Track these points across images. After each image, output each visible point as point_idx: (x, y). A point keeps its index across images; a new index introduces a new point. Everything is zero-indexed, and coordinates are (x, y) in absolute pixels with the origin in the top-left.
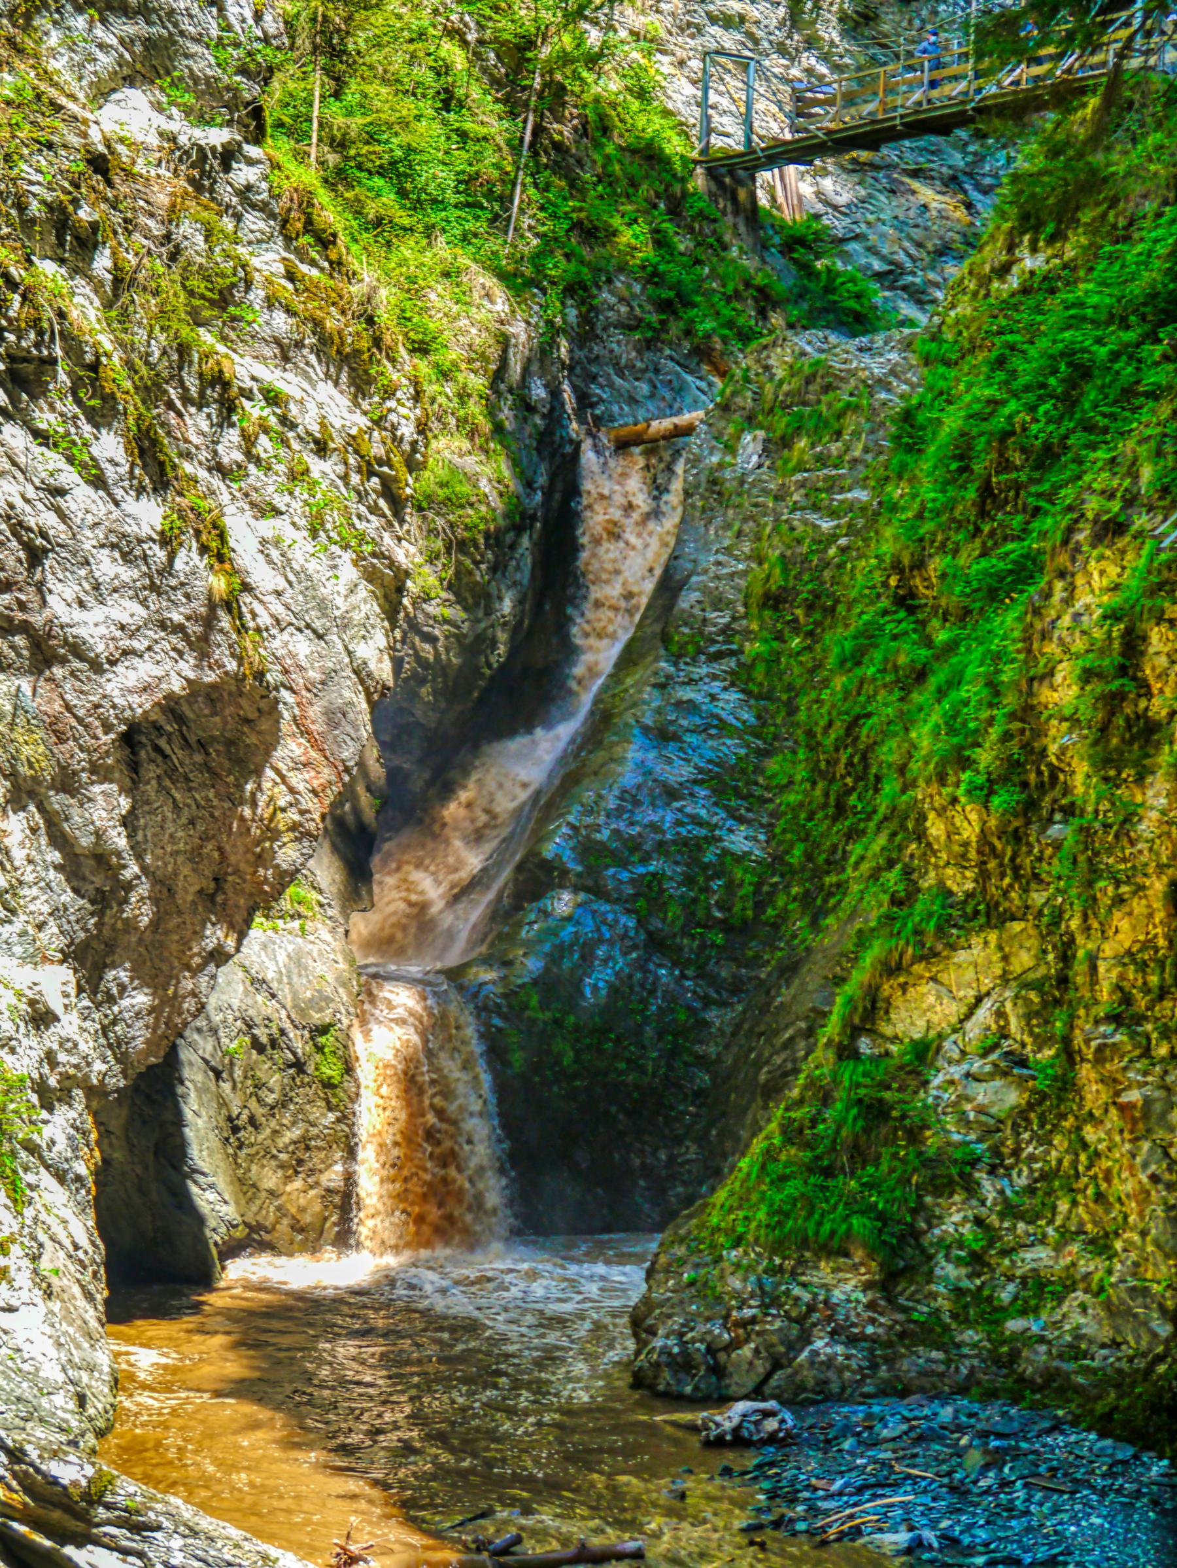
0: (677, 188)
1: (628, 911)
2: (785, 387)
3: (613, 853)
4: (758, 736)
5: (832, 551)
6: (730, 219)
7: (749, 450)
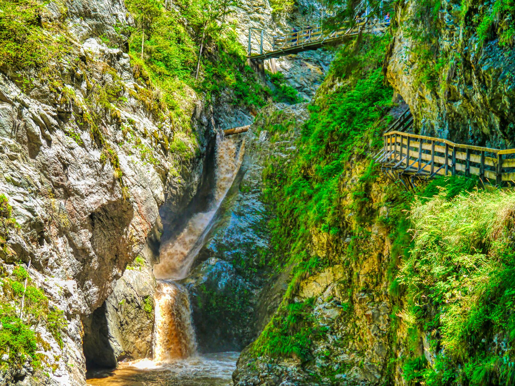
0: (242, 65)
1: (230, 263)
2: (272, 119)
3: (226, 247)
4: (266, 214)
5: (286, 163)
6: (257, 73)
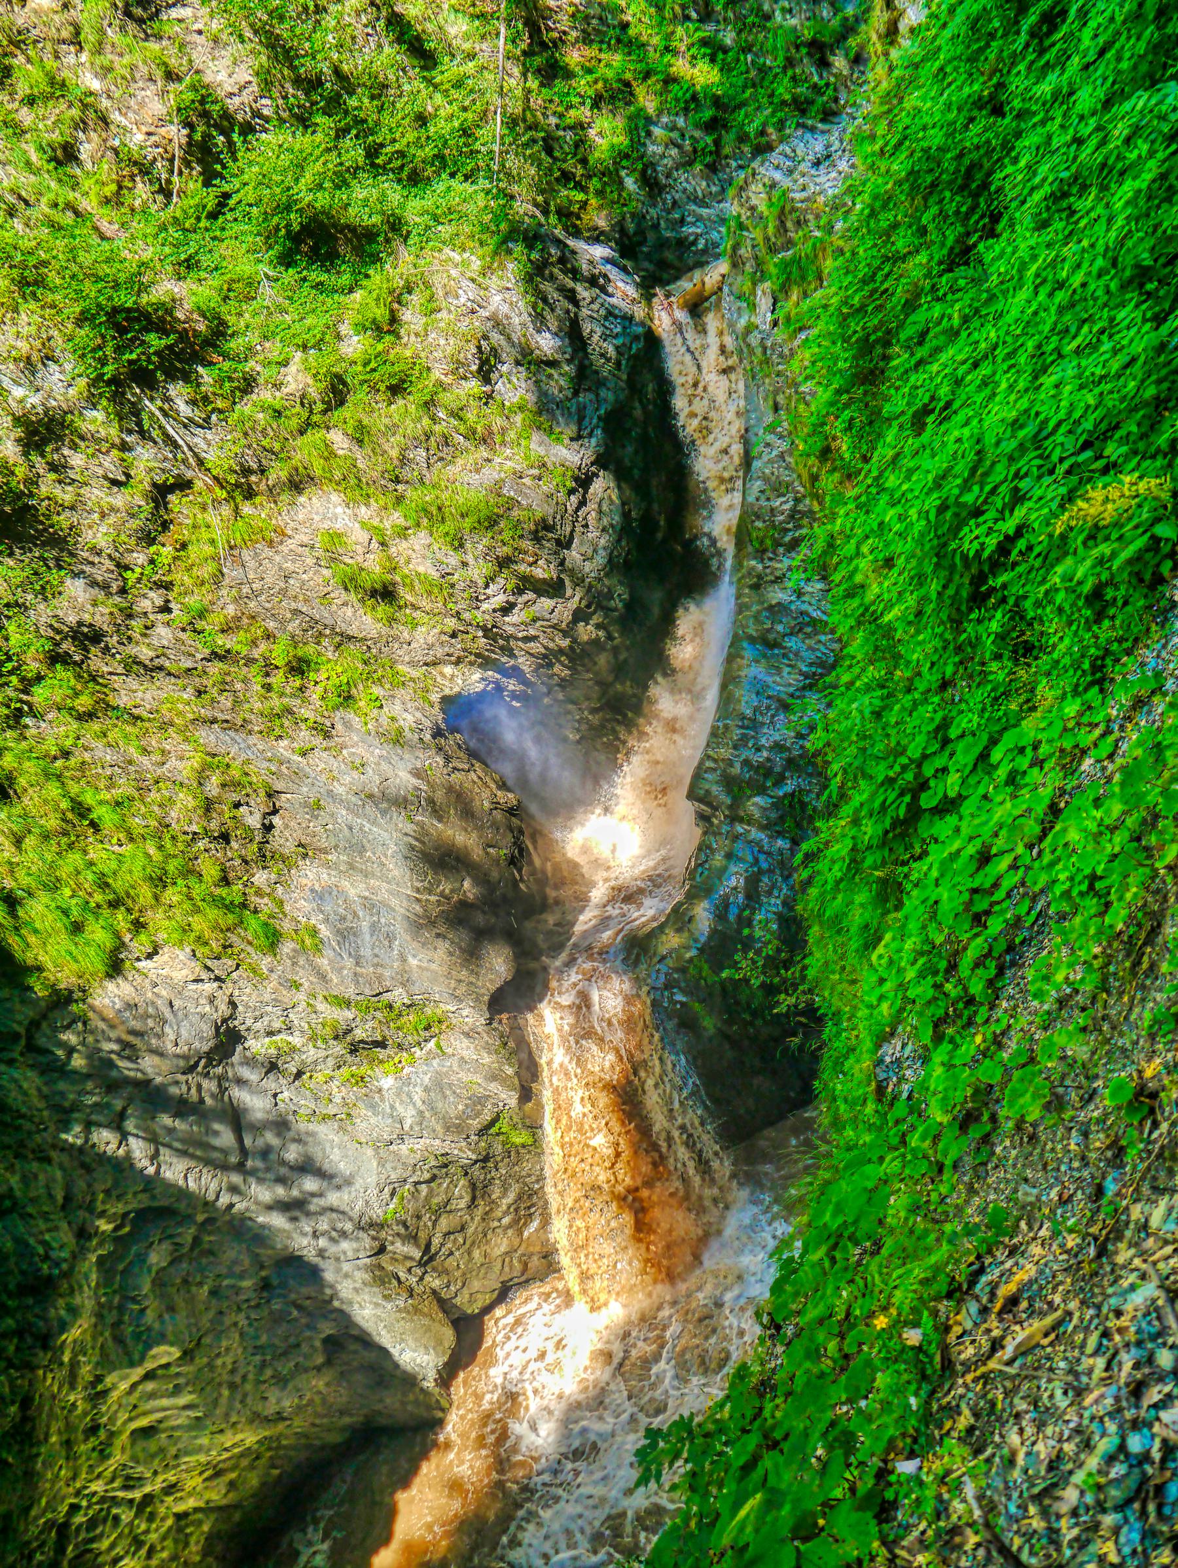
1: (780, 834)
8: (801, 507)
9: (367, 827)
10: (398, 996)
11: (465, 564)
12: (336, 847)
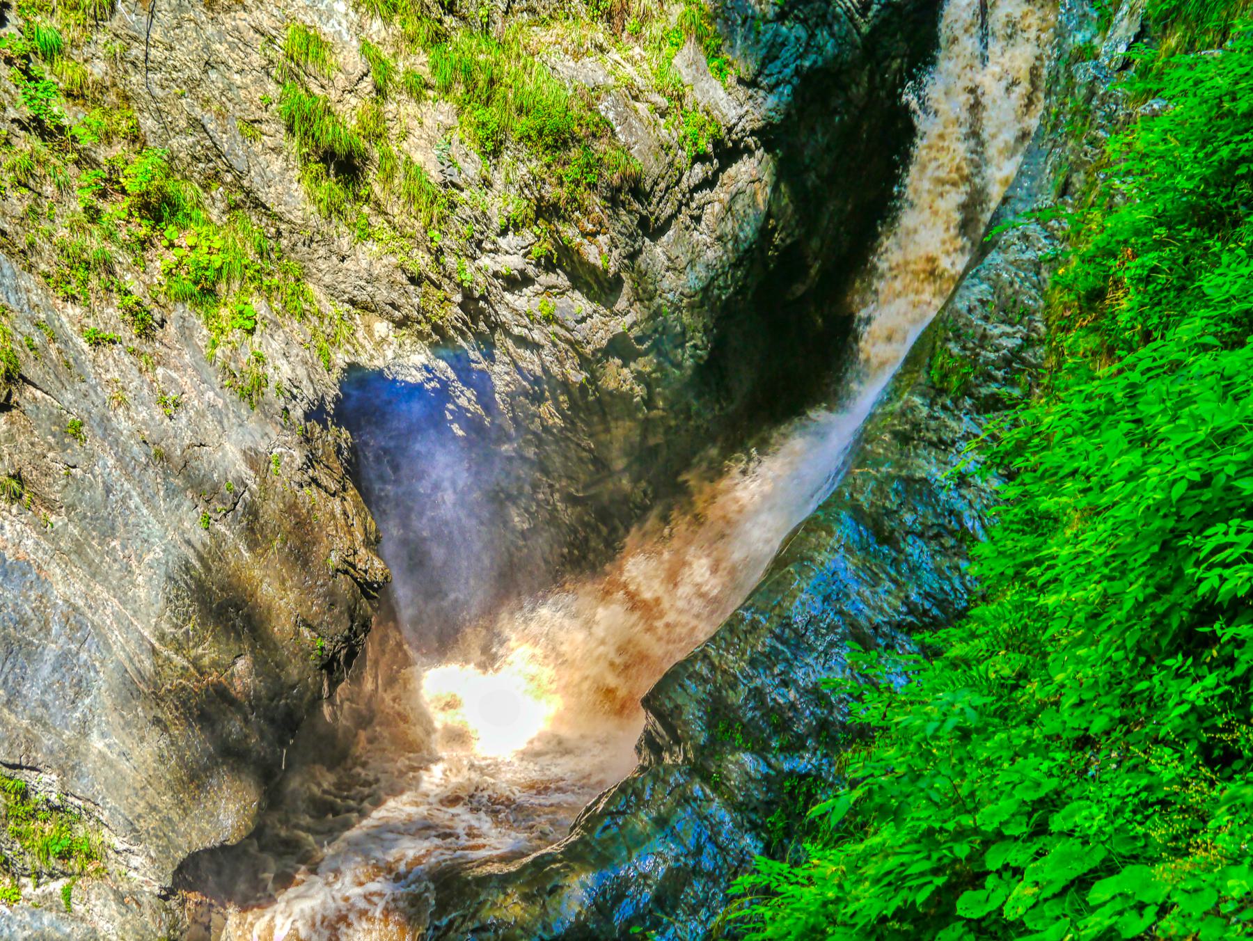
1: (754, 827)
7: (1121, 32)
8: (1027, 355)
9: (135, 500)
10: (46, 785)
11: (487, 183)
12: (71, 507)
